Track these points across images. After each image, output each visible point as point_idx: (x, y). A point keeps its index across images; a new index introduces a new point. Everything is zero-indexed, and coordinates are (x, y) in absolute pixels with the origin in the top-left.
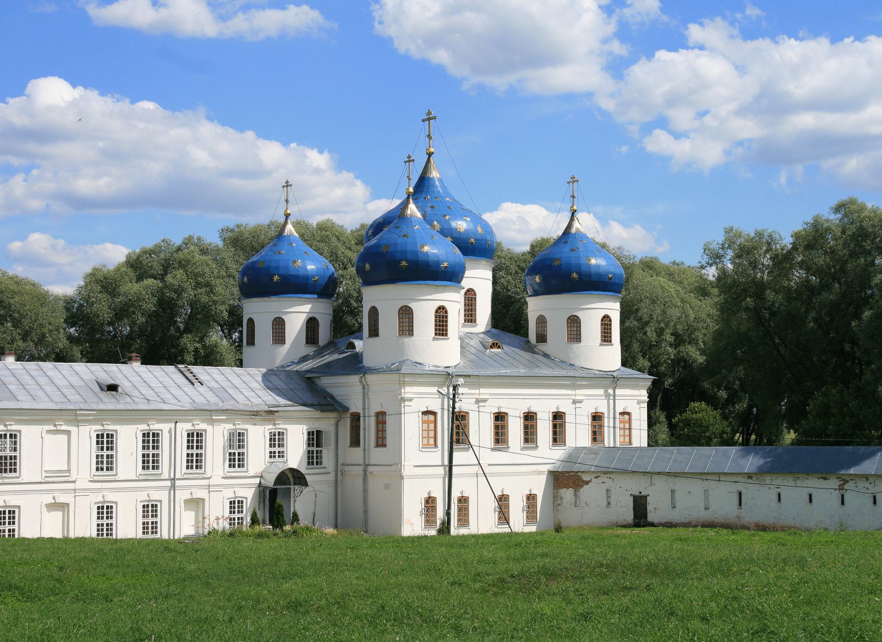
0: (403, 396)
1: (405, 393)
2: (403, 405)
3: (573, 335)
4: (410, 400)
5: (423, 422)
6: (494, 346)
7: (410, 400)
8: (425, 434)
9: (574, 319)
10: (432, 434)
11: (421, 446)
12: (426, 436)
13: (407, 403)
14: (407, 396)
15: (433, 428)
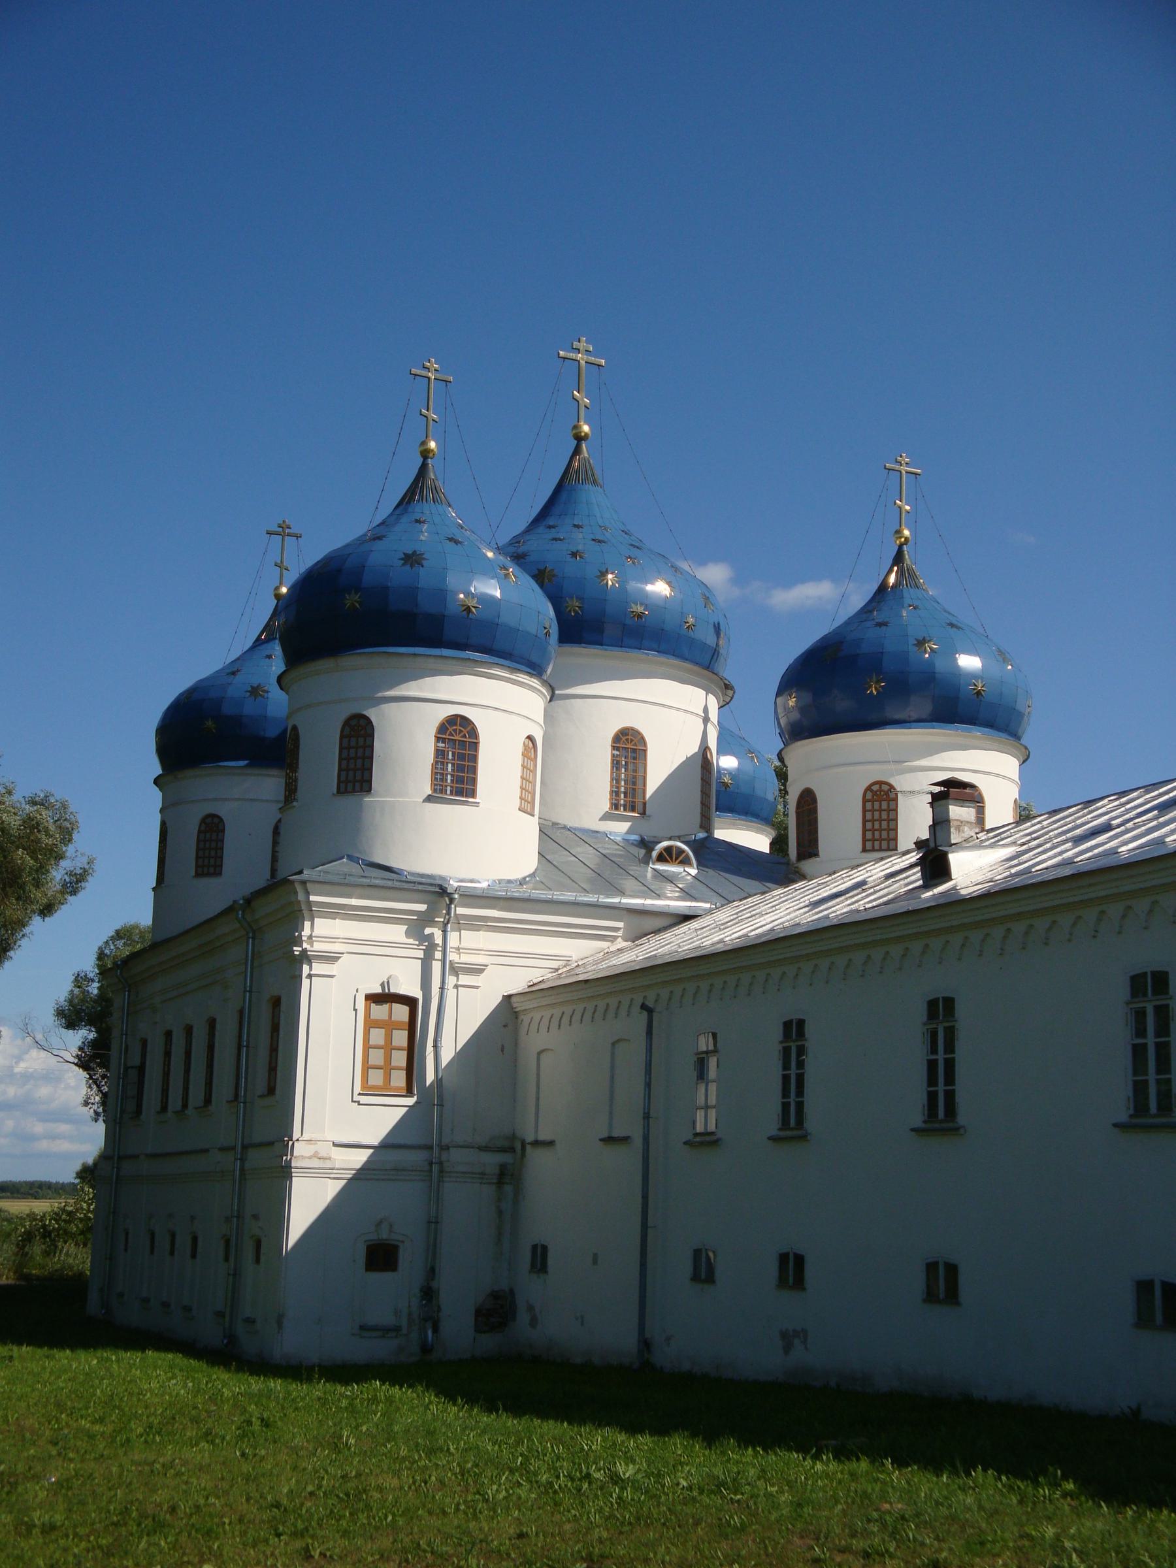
0: (305, 945)
1: (310, 937)
2: (306, 968)
3: (880, 830)
4: (332, 958)
5: (370, 1024)
6: (672, 859)
7: (332, 958)
8: (377, 1057)
9: (881, 790)
10: (400, 1059)
11: (358, 1089)
12: (381, 1062)
13: (318, 968)
14: (317, 946)
15: (405, 1044)
